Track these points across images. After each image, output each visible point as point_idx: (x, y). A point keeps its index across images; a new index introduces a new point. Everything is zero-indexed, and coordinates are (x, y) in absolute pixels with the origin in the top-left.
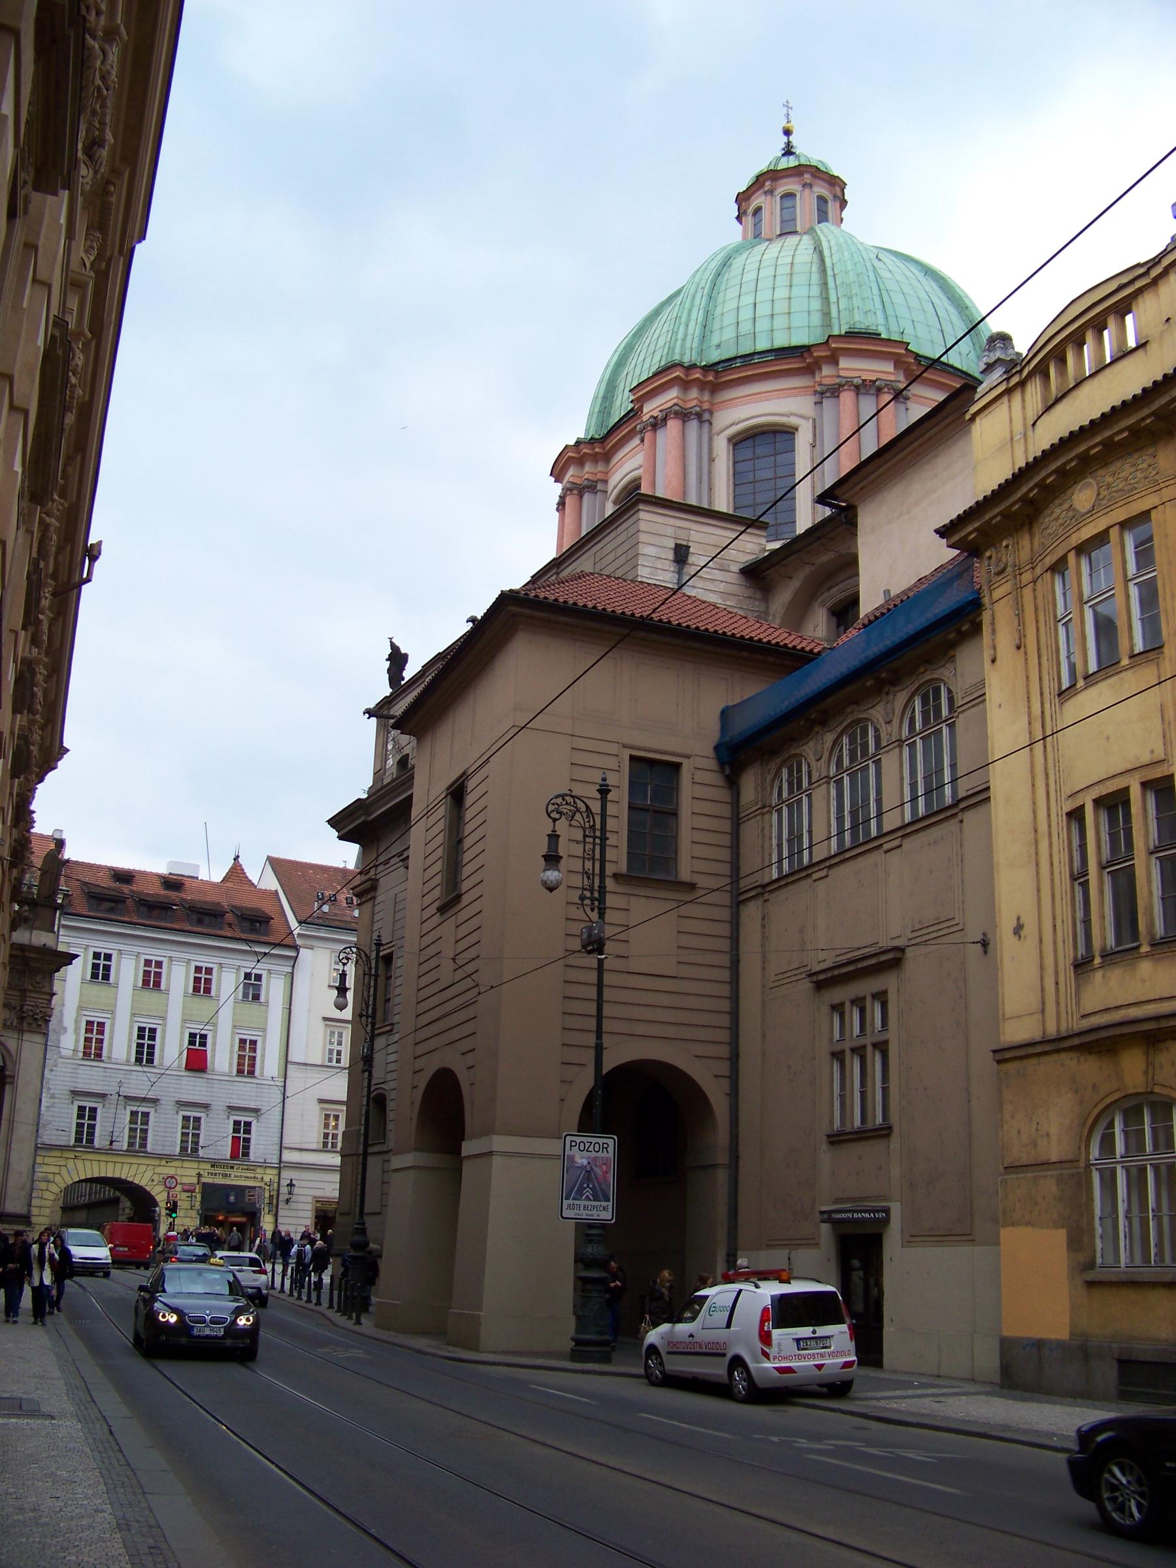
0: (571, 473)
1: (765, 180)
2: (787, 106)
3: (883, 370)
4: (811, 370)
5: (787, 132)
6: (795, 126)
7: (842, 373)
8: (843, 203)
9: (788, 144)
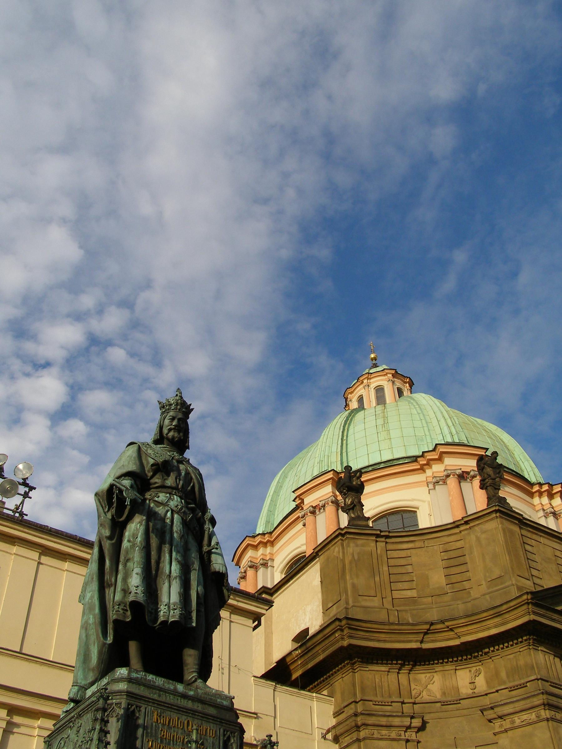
4: (422, 469)
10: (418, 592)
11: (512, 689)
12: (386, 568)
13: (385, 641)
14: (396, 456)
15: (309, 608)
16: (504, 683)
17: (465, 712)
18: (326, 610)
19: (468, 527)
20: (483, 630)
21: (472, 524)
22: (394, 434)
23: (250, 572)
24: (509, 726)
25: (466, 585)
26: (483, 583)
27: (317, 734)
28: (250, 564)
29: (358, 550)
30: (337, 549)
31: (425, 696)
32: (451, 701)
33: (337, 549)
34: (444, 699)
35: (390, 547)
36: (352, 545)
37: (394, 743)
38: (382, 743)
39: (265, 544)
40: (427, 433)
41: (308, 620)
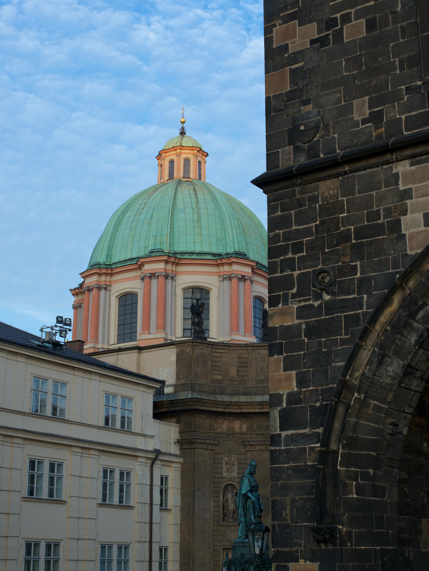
4: (218, 265)
10: (223, 377)
11: (257, 434)
12: (210, 362)
13: (210, 407)
15: (166, 370)
19: (252, 348)
21: (254, 348)
22: (205, 231)
23: (95, 291)
24: (253, 449)
25: (246, 378)
26: (254, 380)
27: (173, 442)
28: (96, 286)
30: (188, 349)
31: (220, 430)
32: (231, 434)
33: (188, 349)
34: (227, 433)
35: (214, 350)
36: (197, 349)
37: (205, 450)
38: (201, 450)
39: (106, 274)
40: (224, 238)
41: (165, 376)
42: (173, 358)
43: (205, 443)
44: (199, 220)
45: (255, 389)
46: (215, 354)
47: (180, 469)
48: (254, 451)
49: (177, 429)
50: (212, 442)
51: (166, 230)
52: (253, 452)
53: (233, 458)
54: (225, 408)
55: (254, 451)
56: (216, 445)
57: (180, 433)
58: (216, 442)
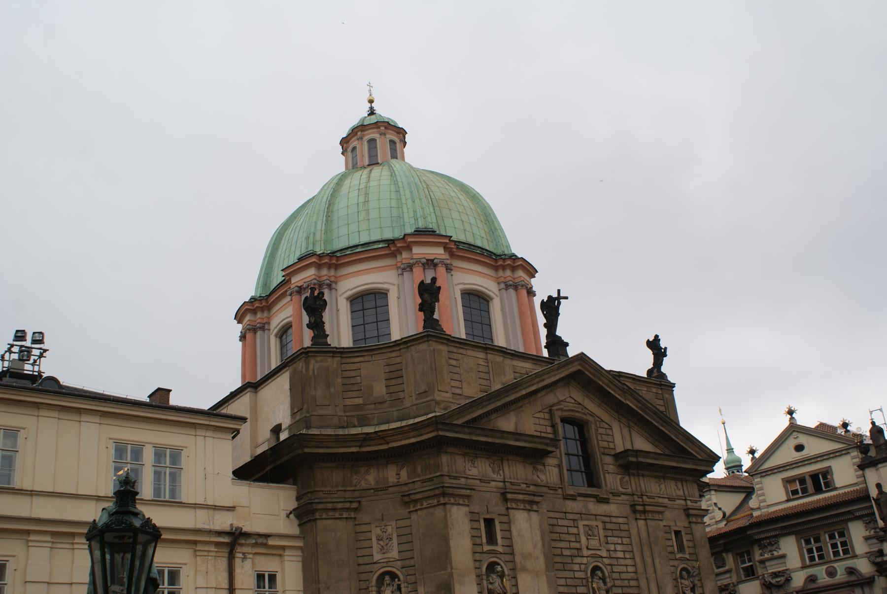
0: (248, 317)
1: (358, 131)
2: (369, 85)
3: (438, 252)
4: (393, 255)
5: (371, 101)
6: (375, 96)
7: (415, 257)
8: (405, 143)
9: (371, 108)
11: (423, 481)
12: (340, 380)
13: (332, 448)
14: (374, 239)
16: (419, 476)
17: (391, 496)
18: (293, 414)
20: (405, 439)
22: (373, 214)
24: (419, 507)
25: (401, 395)
27: (283, 514)
29: (317, 365)
31: (363, 485)
32: (381, 489)
35: (345, 360)
37: (338, 522)
38: (329, 522)
42: (287, 387)
43: (335, 510)
44: (366, 202)
45: (414, 407)
46: (348, 367)
47: (300, 559)
48: (420, 509)
49: (294, 494)
50: (347, 505)
51: (320, 226)
52: (419, 512)
53: (389, 529)
54: (360, 447)
55: (420, 509)
56: (356, 510)
57: (298, 499)
58: (355, 505)
